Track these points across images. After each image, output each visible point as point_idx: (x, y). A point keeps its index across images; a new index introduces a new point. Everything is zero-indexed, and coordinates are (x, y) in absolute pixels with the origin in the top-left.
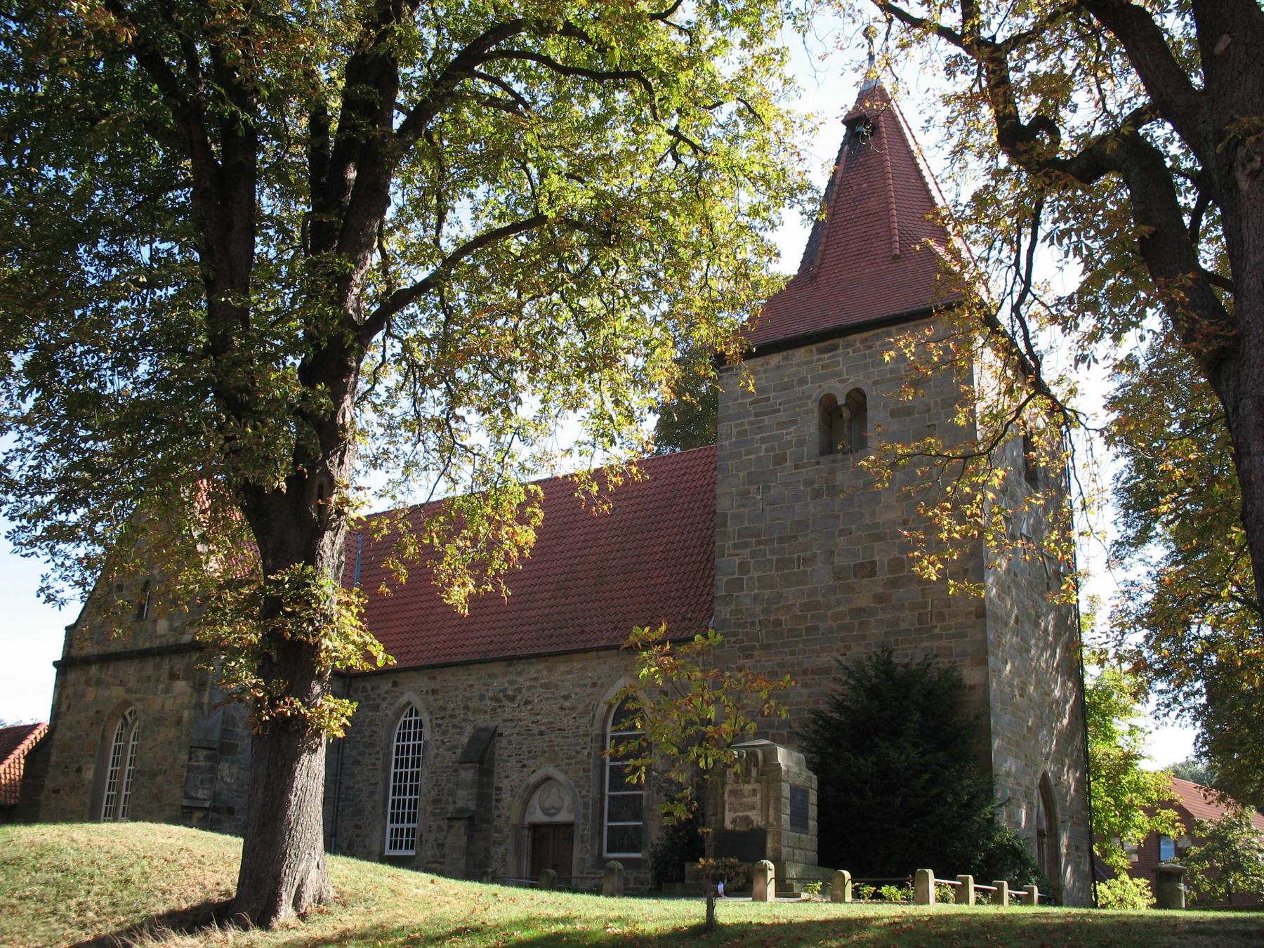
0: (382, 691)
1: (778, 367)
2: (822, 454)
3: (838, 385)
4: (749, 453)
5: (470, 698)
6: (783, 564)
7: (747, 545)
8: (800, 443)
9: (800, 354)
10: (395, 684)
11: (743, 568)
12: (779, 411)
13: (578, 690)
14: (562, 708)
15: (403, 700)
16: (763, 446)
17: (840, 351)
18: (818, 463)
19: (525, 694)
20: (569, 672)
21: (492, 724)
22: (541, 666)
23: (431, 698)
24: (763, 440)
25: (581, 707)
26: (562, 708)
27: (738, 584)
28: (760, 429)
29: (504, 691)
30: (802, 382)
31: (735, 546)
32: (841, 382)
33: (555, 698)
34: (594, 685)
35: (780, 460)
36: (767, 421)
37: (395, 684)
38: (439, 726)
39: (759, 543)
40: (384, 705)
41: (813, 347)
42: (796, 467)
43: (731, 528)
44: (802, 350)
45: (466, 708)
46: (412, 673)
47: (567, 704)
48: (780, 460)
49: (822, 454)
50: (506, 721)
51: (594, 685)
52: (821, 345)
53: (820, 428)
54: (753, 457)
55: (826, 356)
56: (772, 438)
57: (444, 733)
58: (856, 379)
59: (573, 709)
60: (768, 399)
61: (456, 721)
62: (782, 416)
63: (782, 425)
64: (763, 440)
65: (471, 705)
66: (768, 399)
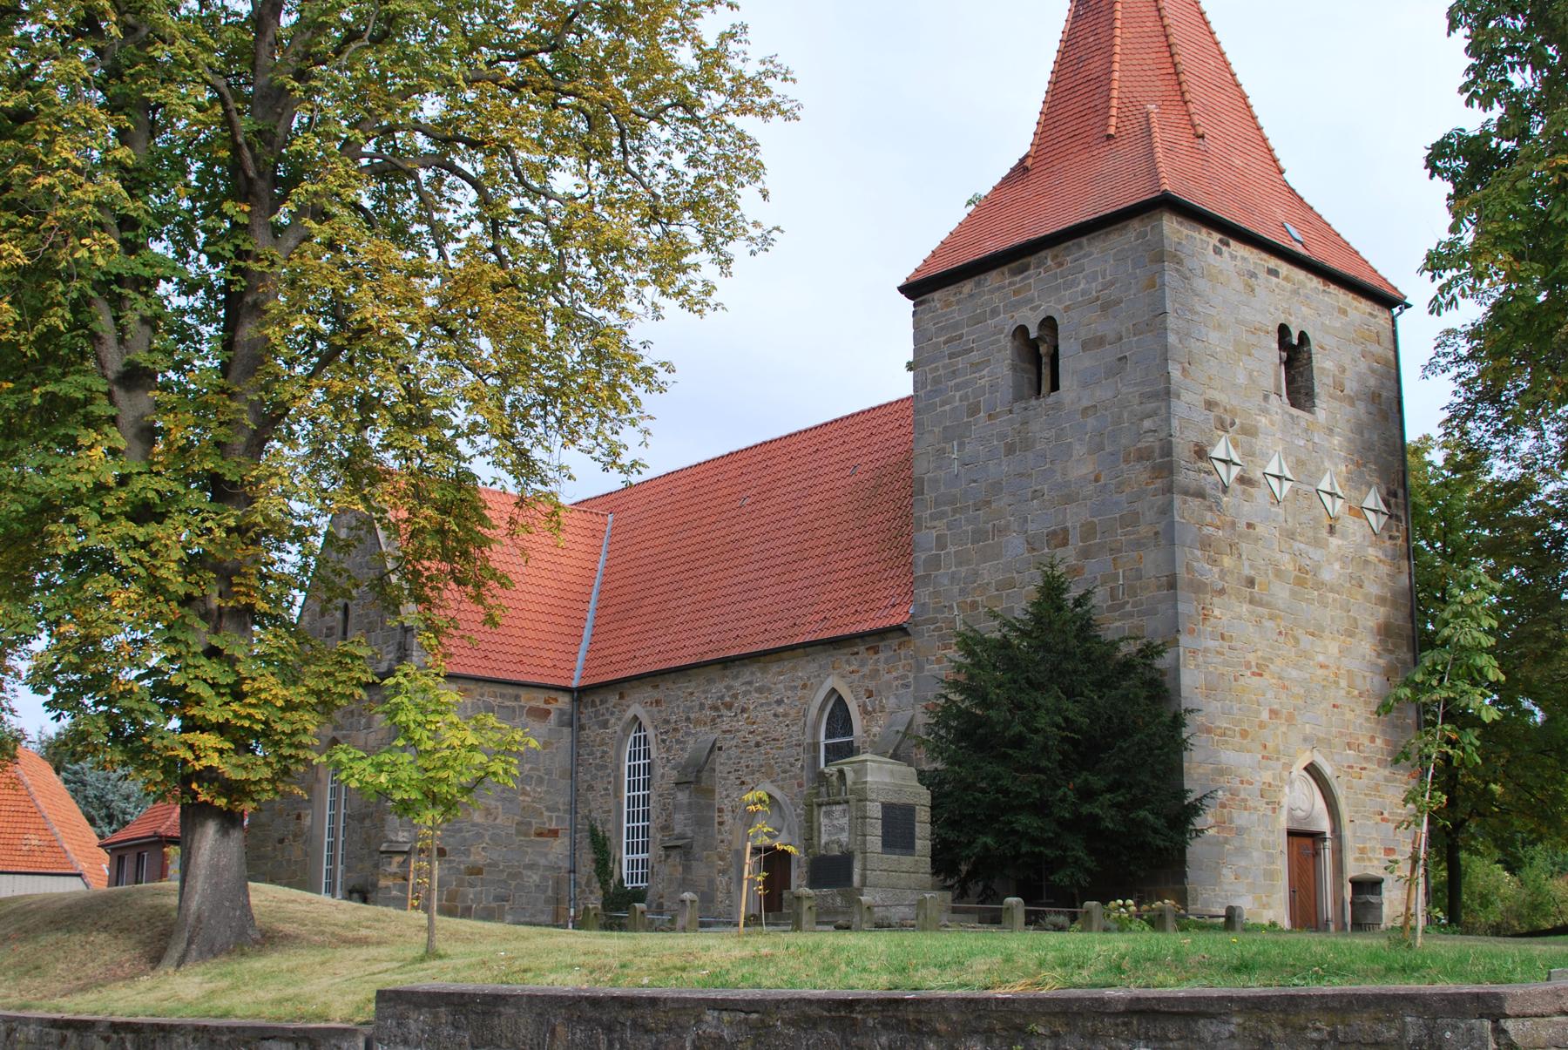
0: (610, 705)
1: (971, 296)
2: (1016, 400)
3: (1029, 313)
4: (944, 403)
5: (691, 708)
6: (979, 535)
7: (943, 515)
8: (993, 387)
9: (993, 279)
10: (622, 696)
11: (941, 543)
12: (972, 350)
13: (789, 693)
14: (775, 715)
15: (629, 714)
16: (958, 395)
18: (1011, 412)
19: (741, 701)
20: (781, 673)
21: (712, 737)
22: (754, 668)
23: (655, 709)
24: (958, 387)
25: (793, 712)
26: (775, 715)
27: (935, 562)
29: (722, 698)
30: (995, 312)
31: (933, 517)
32: (1033, 309)
33: (769, 704)
34: (804, 686)
35: (974, 410)
36: (960, 362)
37: (622, 696)
38: (664, 741)
39: (955, 511)
40: (613, 721)
41: (1005, 269)
43: (929, 495)
44: (994, 273)
45: (688, 719)
47: (781, 710)
49: (1016, 400)
50: (725, 732)
51: (804, 686)
52: (1013, 265)
53: (1014, 368)
54: (947, 407)
55: (1018, 278)
56: (966, 384)
57: (668, 750)
59: (785, 715)
60: (961, 337)
61: (679, 735)
62: (975, 356)
63: (976, 367)
64: (958, 387)
65: (692, 716)
66: (961, 337)
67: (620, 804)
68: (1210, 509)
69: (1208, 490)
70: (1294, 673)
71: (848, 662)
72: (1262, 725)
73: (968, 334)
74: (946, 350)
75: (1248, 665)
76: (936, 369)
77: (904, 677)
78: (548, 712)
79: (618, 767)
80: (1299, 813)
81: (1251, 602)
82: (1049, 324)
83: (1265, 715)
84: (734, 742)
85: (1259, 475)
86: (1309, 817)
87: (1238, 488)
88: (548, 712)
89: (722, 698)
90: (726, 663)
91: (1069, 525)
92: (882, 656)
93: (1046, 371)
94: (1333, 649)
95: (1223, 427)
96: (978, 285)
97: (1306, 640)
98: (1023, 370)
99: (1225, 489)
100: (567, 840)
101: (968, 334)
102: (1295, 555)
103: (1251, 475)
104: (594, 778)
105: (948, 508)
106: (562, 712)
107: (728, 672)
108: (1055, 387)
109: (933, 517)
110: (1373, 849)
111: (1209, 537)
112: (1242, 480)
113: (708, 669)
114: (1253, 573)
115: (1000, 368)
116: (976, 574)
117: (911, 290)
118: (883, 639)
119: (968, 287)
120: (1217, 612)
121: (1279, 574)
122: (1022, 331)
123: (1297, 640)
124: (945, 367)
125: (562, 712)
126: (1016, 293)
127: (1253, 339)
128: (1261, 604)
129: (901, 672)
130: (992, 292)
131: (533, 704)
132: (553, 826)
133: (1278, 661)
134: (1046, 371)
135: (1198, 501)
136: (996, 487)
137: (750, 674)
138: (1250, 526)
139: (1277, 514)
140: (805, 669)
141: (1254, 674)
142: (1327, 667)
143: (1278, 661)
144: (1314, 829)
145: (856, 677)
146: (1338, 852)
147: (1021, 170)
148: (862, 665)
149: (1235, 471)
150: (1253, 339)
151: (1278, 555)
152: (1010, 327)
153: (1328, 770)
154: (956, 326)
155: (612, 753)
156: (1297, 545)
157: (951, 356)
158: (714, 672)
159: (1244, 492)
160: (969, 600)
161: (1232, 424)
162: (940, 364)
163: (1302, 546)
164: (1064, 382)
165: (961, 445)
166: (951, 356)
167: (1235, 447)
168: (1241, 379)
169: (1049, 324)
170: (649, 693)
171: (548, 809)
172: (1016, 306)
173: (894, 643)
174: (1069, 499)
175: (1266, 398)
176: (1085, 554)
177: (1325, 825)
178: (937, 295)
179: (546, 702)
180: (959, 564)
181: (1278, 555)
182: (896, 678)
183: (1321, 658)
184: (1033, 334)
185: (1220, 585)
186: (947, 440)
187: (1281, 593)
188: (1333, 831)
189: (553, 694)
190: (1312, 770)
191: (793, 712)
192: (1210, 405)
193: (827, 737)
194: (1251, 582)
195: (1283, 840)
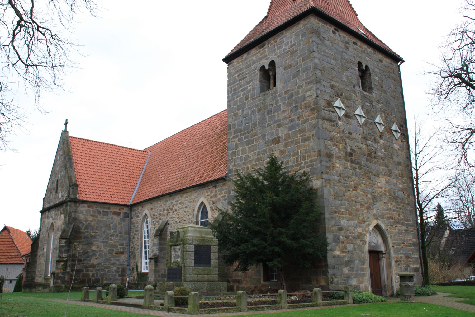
0: (139, 210)
1: (246, 59)
2: (261, 92)
5: (161, 210)
7: (237, 136)
8: (254, 89)
9: (253, 51)
10: (142, 207)
11: (236, 147)
12: (246, 77)
13: (189, 204)
14: (185, 212)
15: (144, 213)
16: (242, 93)
17: (266, 46)
18: (259, 97)
19: (175, 207)
20: (187, 197)
21: (166, 220)
22: (179, 196)
23: (151, 211)
24: (242, 91)
25: (190, 211)
26: (185, 212)
27: (234, 154)
28: (241, 86)
29: (169, 206)
30: (254, 63)
31: (234, 138)
32: (267, 59)
33: (183, 208)
34: (194, 201)
35: (247, 98)
36: (243, 82)
37: (142, 207)
38: (153, 222)
39: (241, 135)
40: (140, 215)
41: (257, 47)
42: (253, 99)
45: (160, 214)
46: (146, 203)
47: (186, 210)
48: (247, 98)
50: (170, 218)
51: (194, 201)
53: (260, 81)
54: (238, 98)
55: (261, 50)
56: (244, 89)
57: (155, 225)
58: (272, 57)
59: (188, 212)
60: (243, 73)
61: (158, 220)
63: (248, 83)
64: (242, 91)
65: (161, 213)
66: (243, 73)
67: (141, 244)
70: (369, 190)
71: (207, 192)
73: (245, 72)
74: (238, 79)
76: (235, 86)
77: (225, 196)
78: (120, 213)
79: (141, 231)
80: (373, 244)
82: (272, 64)
84: (173, 222)
86: (377, 246)
88: (120, 213)
89: (169, 206)
90: (171, 194)
91: (280, 135)
92: (217, 189)
93: (272, 81)
95: (338, 96)
96: (248, 54)
98: (264, 82)
99: (340, 118)
100: (127, 255)
101: (245, 72)
104: (135, 234)
105: (239, 134)
106: (125, 213)
107: (171, 198)
108: (275, 85)
109: (234, 138)
110: (401, 258)
112: (346, 115)
113: (166, 197)
115: (256, 82)
116: (248, 156)
117: (228, 60)
118: (218, 183)
119: (245, 56)
122: (263, 67)
124: (238, 84)
125: (125, 213)
126: (261, 55)
127: (348, 65)
129: (223, 195)
130: (253, 56)
131: (115, 210)
132: (122, 251)
133: (363, 185)
134: (272, 81)
136: (255, 124)
137: (179, 198)
138: (350, 133)
140: (193, 195)
143: (363, 185)
144: (379, 250)
145: (209, 197)
146: (389, 258)
147: (266, 17)
148: (211, 192)
149: (343, 112)
150: (348, 65)
152: (259, 67)
153: (383, 226)
154: (241, 70)
155: (140, 226)
157: (240, 80)
158: (167, 198)
159: (347, 120)
160: (246, 167)
161: (342, 95)
162: (236, 84)
164: (277, 84)
165: (243, 111)
166: (240, 80)
167: (343, 103)
168: (344, 79)
169: (272, 64)
170: (149, 206)
171: (120, 245)
172: (260, 59)
173: (221, 184)
174: (279, 126)
176: (286, 145)
177: (383, 248)
178: (235, 60)
179: (120, 210)
180: (242, 154)
182: (222, 197)
184: (267, 68)
186: (238, 109)
188: (386, 250)
189: (122, 207)
190: (377, 227)
191: (190, 211)
193: (201, 219)
195: (367, 255)
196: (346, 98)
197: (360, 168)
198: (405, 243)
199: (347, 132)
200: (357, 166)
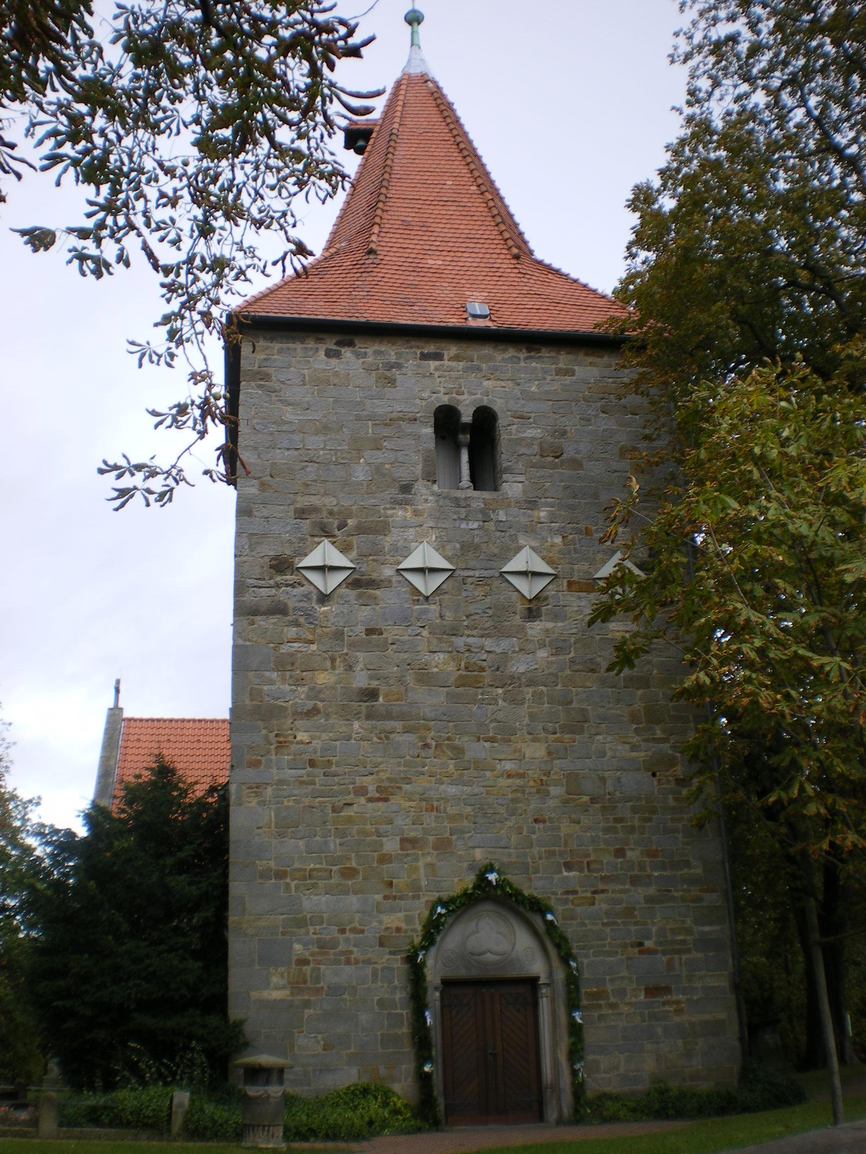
68: (297, 624)
69: (291, 604)
70: (452, 790)
72: (384, 859)
75: (361, 791)
81: (368, 717)
83: (391, 846)
85: (388, 572)
87: (351, 594)
94: (536, 751)
97: (477, 750)
99: (324, 598)
102: (455, 653)
103: (374, 576)
111: (291, 655)
114: (374, 684)
120: (302, 736)
121: (425, 677)
123: (458, 752)
128: (389, 716)
135: (273, 619)
138: (370, 632)
139: (425, 612)
141: (370, 800)
142: (522, 776)
151: (427, 657)
156: (459, 642)
163: (470, 640)
175: (406, 488)
181: (427, 657)
183: (509, 766)
185: (310, 704)
187: (430, 701)
192: (301, 513)
194: (371, 694)
196: (361, 530)
197: (407, 730)
198: (649, 944)
199: (360, 629)
200: (398, 725)
